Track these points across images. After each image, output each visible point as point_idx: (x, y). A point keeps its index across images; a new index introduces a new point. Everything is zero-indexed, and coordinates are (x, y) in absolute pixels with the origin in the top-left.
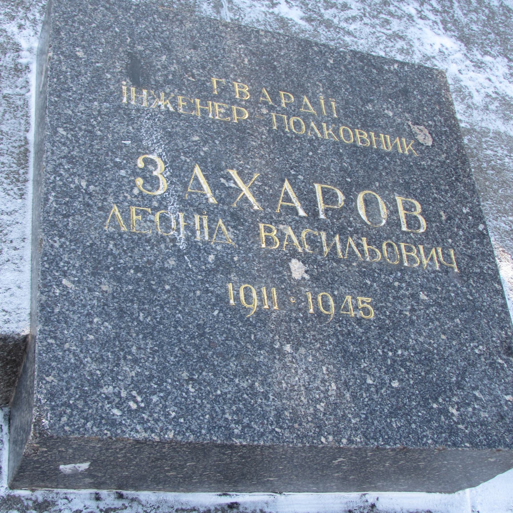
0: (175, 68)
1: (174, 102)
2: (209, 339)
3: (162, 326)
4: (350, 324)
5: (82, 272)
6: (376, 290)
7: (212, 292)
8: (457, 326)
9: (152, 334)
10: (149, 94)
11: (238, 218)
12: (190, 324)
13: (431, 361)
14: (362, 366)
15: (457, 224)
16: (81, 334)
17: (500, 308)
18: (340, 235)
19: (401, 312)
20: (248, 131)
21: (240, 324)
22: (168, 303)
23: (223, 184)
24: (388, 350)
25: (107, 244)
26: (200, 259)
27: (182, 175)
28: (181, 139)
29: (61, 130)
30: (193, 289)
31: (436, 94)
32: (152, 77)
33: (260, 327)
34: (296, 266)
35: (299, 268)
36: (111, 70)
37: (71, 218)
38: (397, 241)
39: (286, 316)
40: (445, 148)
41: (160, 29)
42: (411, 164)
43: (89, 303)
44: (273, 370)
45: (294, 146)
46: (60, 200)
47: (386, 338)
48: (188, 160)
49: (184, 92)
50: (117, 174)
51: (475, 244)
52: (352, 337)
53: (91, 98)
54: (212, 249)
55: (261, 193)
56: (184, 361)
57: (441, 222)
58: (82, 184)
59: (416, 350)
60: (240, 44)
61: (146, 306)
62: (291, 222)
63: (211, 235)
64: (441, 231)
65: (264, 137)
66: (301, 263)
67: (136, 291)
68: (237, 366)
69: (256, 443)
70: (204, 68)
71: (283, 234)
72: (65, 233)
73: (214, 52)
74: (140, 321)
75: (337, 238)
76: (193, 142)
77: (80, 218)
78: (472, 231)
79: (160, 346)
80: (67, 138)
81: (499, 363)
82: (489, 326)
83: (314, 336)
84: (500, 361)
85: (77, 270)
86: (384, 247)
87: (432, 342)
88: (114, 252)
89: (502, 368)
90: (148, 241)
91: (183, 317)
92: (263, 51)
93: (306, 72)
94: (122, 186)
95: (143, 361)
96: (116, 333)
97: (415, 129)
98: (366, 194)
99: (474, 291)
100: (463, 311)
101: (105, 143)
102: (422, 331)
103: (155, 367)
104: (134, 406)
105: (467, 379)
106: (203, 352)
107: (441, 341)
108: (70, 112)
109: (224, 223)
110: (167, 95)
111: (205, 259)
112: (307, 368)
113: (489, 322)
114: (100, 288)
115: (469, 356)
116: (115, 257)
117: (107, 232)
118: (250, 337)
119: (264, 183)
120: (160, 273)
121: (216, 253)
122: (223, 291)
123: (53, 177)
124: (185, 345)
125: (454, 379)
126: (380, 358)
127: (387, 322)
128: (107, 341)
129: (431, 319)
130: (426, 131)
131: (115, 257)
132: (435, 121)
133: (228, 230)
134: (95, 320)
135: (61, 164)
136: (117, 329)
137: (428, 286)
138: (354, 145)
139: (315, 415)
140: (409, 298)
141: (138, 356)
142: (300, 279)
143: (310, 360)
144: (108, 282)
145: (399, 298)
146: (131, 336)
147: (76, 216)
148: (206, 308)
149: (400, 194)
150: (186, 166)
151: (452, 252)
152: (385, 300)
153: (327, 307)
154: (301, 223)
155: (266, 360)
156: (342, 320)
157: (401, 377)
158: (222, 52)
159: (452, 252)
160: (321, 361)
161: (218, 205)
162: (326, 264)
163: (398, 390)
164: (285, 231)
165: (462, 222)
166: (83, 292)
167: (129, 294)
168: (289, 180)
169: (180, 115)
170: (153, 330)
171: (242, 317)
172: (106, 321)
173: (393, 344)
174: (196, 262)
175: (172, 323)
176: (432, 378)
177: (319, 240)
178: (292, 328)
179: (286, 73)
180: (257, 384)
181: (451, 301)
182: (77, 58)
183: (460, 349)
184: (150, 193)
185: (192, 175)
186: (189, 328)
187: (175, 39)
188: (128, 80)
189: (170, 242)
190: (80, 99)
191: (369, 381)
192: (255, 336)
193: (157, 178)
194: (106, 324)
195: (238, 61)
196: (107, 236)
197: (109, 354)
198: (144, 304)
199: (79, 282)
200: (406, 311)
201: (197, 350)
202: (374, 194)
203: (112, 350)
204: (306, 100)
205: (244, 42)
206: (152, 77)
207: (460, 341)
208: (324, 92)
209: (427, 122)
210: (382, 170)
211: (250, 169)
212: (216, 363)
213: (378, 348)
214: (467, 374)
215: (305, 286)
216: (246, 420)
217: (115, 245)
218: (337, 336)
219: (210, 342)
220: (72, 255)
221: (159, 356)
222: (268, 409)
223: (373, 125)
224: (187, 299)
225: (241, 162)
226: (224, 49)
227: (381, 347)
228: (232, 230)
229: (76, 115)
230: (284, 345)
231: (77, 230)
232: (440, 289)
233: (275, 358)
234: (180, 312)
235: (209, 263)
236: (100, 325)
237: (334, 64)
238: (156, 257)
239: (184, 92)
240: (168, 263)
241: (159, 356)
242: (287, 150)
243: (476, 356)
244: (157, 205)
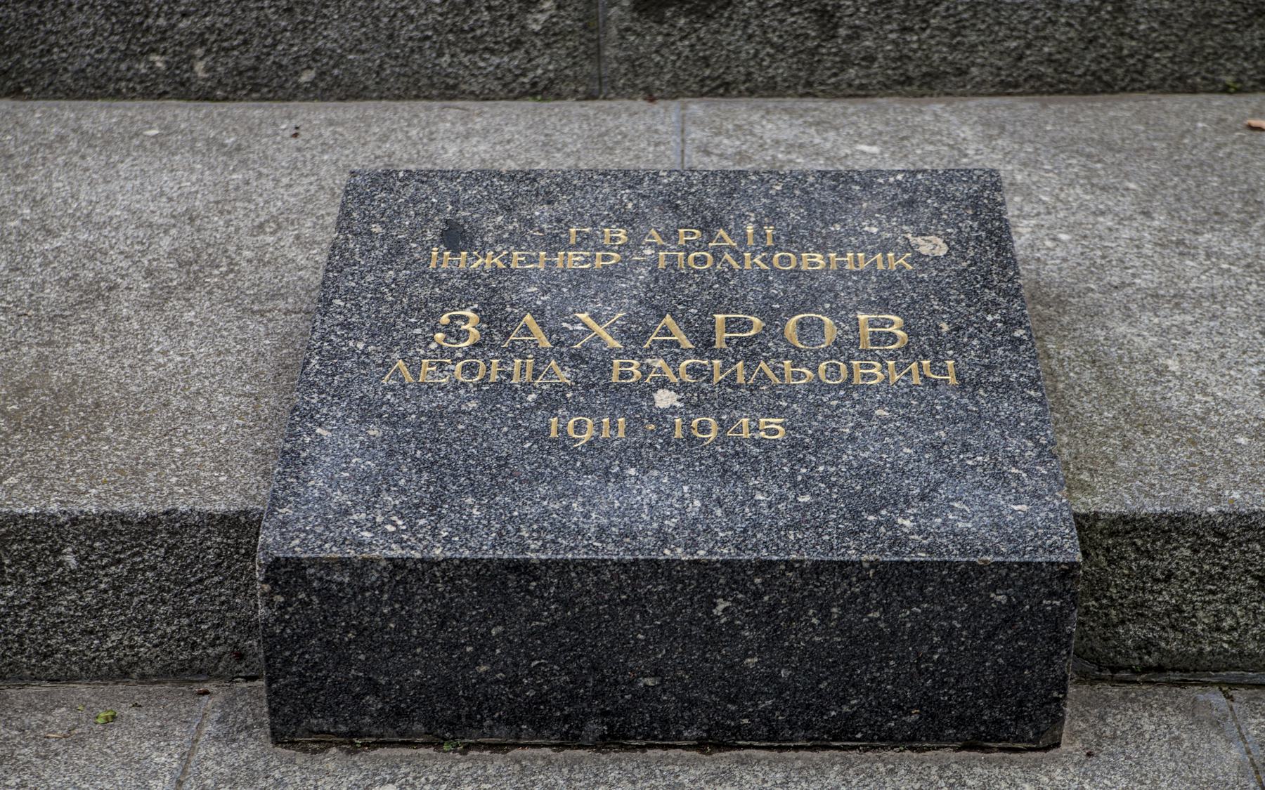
1: (507, 259)
7: (526, 428)
10: (470, 255)
29: (338, 302)
34: (664, 396)
55: (624, 332)
63: (535, 377)
69: (559, 557)
84: (1014, 470)
86: (823, 366)
89: (1018, 477)
90: (442, 389)
101: (398, 307)
104: (390, 528)
110: (496, 254)
116: (392, 406)
130: (940, 241)
132: (959, 228)
138: (797, 269)
139: (659, 530)
149: (866, 312)
153: (704, 428)
163: (807, 505)
180: (574, 505)
182: (370, 233)
191: (759, 497)
204: (722, 232)
205: (630, 187)
216: (549, 537)
222: (586, 526)
226: (596, 199)
232: (914, 403)
238: (450, 402)
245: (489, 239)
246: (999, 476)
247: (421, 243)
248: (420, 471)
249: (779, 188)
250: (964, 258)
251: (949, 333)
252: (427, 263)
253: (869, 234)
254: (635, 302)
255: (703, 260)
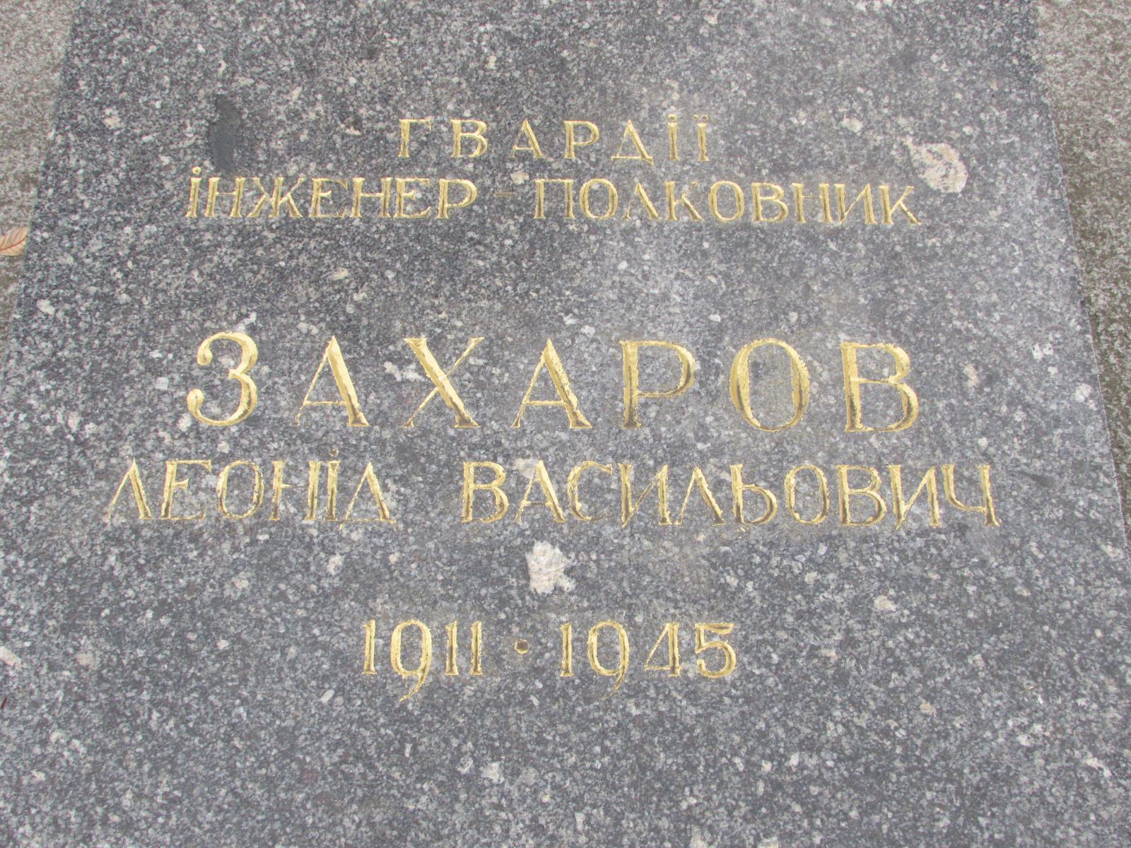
0: (318, 114)
1: (303, 196)
2: (302, 763)
3: (196, 740)
4: (667, 697)
5: (43, 625)
6: (750, 601)
7: (325, 647)
8: (974, 673)
9: (172, 760)
11: (414, 455)
12: (262, 728)
13: (881, 776)
14: (684, 805)
15: (1010, 394)
16: (18, 770)
17: (1113, 613)
18: (672, 465)
19: (813, 652)
20: (471, 234)
21: (382, 720)
22: (221, 682)
23: (391, 376)
24: (763, 757)
25: (104, 557)
26: (308, 569)
27: (296, 367)
28: (306, 282)
29: (45, 306)
30: (282, 642)
31: (992, 50)
32: (263, 144)
33: (430, 724)
34: (544, 560)
35: (550, 564)
36: (172, 147)
37: (36, 504)
38: (828, 462)
39: (499, 690)
40: (1003, 190)
41: (297, 28)
42: (898, 248)
43: (47, 697)
44: (446, 831)
45: (582, 255)
46: (19, 465)
47: (762, 725)
48: (315, 331)
49: (330, 167)
50: (150, 388)
51: (1057, 441)
52: (666, 731)
53: (118, 219)
54: (341, 539)
55: (480, 386)
56: (235, 820)
57: (964, 394)
58: (70, 422)
59: (842, 751)
60: (483, 24)
61: (169, 695)
62: (545, 449)
64: (960, 417)
65: (508, 242)
66: (557, 551)
67: (152, 660)
68: (359, 825)
70: (385, 100)
71: (522, 482)
72: (19, 541)
73: (416, 56)
74: (150, 730)
75: (663, 473)
76: (333, 283)
77: (55, 503)
78: (1054, 407)
79: (187, 788)
80: (55, 320)
81: (1089, 769)
82: (1070, 667)
83: (565, 735)
84: (1092, 762)
85: (33, 623)
86: (791, 479)
87: (893, 724)
88: (116, 573)
91: (249, 713)
92: (538, 30)
93: (641, 61)
94: (163, 411)
95: (143, 825)
96: (94, 763)
97: (921, 154)
98: (757, 350)
99: (1037, 572)
100: (996, 631)
101: (134, 319)
102: (868, 697)
103: (168, 839)
105: (983, 821)
106: (282, 795)
107: (918, 719)
108: (70, 260)
109: (378, 474)
110: (289, 181)
111: (319, 566)
112: (535, 819)
113: (1072, 655)
114: (75, 660)
115: (999, 755)
116: (116, 584)
117: (109, 528)
118: (400, 751)
119: (492, 358)
120: (212, 613)
121: (347, 549)
122: (352, 641)
123: (12, 414)
124: (244, 781)
125: (944, 822)
126: (736, 779)
127: (770, 681)
128: (70, 785)
129: (898, 662)
130: (953, 156)
131: (116, 584)
132: (981, 124)
133: (385, 488)
134: (54, 737)
135: (33, 383)
136: (97, 753)
137: (903, 571)
140: (842, 612)
141: (133, 815)
142: (549, 591)
143: (546, 799)
144: (95, 645)
145: (811, 613)
146: (126, 768)
147: (48, 498)
148: (305, 688)
150: (308, 345)
151: (985, 472)
152: (772, 624)
153: (608, 656)
154: (573, 447)
155: (432, 807)
156: (647, 688)
157: (789, 827)
158: (436, 50)
159: (985, 472)
160: (574, 800)
161: (370, 429)
162: (622, 547)
164: (528, 475)
165: (1025, 387)
166: (37, 674)
167: (134, 668)
168: (555, 341)
169: (312, 223)
170: (177, 751)
171: (389, 700)
172: (77, 737)
173: (778, 740)
174: (299, 576)
175: (222, 730)
176: (879, 825)
177: (614, 486)
178: (512, 720)
179: (588, 72)
181: (968, 606)
182: (103, 131)
183: (973, 737)
184: (215, 422)
185: (318, 366)
186: (258, 738)
187: (328, 44)
188: (207, 163)
189: (245, 534)
190: (96, 227)
192: (414, 748)
193: (237, 384)
194: (76, 743)
195: (472, 65)
196: (108, 538)
197: (73, 813)
198: (164, 689)
199: (32, 650)
200: (828, 647)
201: (269, 791)
202: (783, 344)
203: (79, 804)
204: (630, 127)
205: (494, 18)
206: (263, 144)
207: (977, 714)
208: (682, 103)
209: (959, 129)
210: (814, 278)
211: (461, 330)
212: (310, 820)
213: (735, 754)
214: (985, 805)
215: (559, 609)
217: (121, 556)
218: (627, 731)
219: (303, 770)
220: (28, 589)
221: (180, 811)
223: (806, 163)
224: (264, 668)
225: (444, 315)
227: (743, 751)
228: (393, 487)
229: (83, 264)
230: (485, 764)
231: (45, 530)
232: (935, 577)
233: (457, 799)
234: (244, 701)
235: (328, 575)
236: (63, 746)
237: (717, 26)
239: (330, 167)
240: (233, 584)
241: (180, 811)
242: (563, 267)
243: (1020, 753)
244: (226, 451)
245: (279, 145)
246: (1070, 777)
247: (174, 154)
248: (156, 768)
249: (712, 21)
250: (991, 198)
251: (979, 390)
252: (181, 208)
253: (851, 136)
254: (498, 307)
255: (598, 198)
